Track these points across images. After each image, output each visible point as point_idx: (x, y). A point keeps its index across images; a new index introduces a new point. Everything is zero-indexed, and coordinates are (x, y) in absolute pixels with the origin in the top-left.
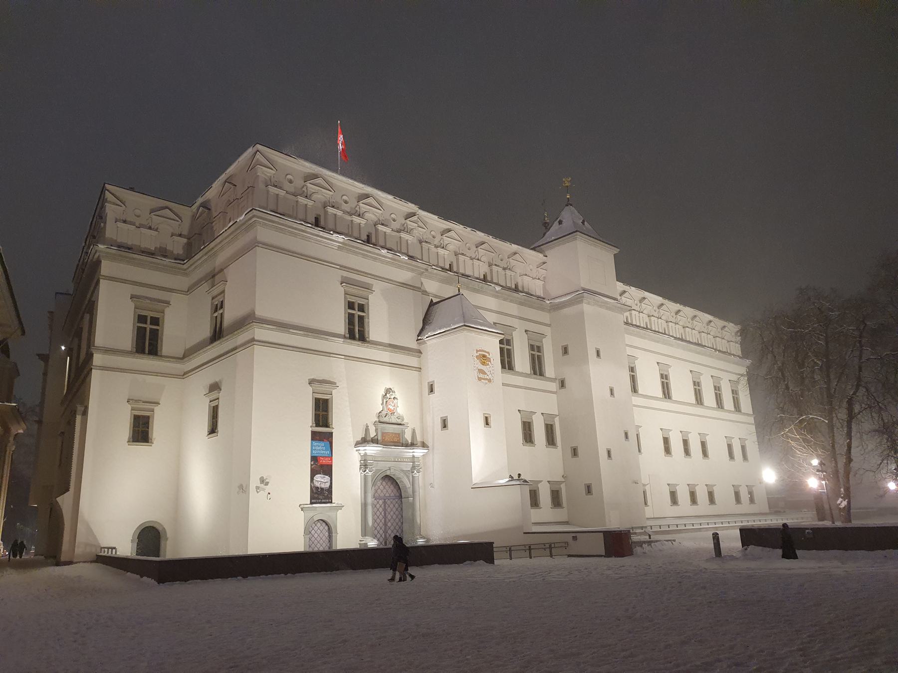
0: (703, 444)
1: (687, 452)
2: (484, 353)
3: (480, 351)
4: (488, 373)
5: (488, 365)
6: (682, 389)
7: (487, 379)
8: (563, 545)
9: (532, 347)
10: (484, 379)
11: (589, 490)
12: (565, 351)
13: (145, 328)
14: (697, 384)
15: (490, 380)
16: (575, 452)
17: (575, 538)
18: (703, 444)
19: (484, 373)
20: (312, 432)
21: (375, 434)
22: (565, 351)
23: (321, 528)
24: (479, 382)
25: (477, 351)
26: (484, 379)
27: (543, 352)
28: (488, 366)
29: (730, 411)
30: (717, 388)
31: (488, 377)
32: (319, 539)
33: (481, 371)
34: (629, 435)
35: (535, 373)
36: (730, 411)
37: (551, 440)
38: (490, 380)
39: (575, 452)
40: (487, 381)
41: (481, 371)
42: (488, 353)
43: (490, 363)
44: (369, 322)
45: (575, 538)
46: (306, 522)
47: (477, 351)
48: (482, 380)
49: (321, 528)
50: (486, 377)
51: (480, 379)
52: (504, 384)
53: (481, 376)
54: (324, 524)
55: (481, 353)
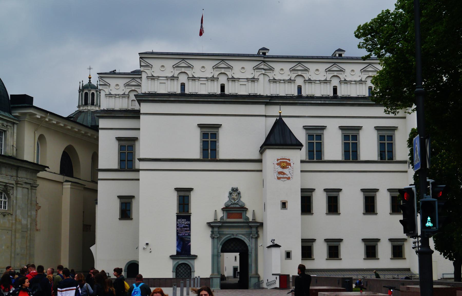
5: (288, 168)
15: (289, 178)
19: (284, 174)
20: (177, 215)
21: (222, 215)
23: (185, 267)
24: (278, 181)
25: (278, 160)
27: (395, 140)
28: (288, 169)
31: (287, 176)
32: (183, 273)
40: (286, 179)
42: (289, 160)
43: (289, 167)
44: (218, 145)
46: (174, 265)
47: (278, 160)
48: (282, 179)
50: (285, 176)
51: (279, 178)
53: (281, 176)
55: (280, 161)
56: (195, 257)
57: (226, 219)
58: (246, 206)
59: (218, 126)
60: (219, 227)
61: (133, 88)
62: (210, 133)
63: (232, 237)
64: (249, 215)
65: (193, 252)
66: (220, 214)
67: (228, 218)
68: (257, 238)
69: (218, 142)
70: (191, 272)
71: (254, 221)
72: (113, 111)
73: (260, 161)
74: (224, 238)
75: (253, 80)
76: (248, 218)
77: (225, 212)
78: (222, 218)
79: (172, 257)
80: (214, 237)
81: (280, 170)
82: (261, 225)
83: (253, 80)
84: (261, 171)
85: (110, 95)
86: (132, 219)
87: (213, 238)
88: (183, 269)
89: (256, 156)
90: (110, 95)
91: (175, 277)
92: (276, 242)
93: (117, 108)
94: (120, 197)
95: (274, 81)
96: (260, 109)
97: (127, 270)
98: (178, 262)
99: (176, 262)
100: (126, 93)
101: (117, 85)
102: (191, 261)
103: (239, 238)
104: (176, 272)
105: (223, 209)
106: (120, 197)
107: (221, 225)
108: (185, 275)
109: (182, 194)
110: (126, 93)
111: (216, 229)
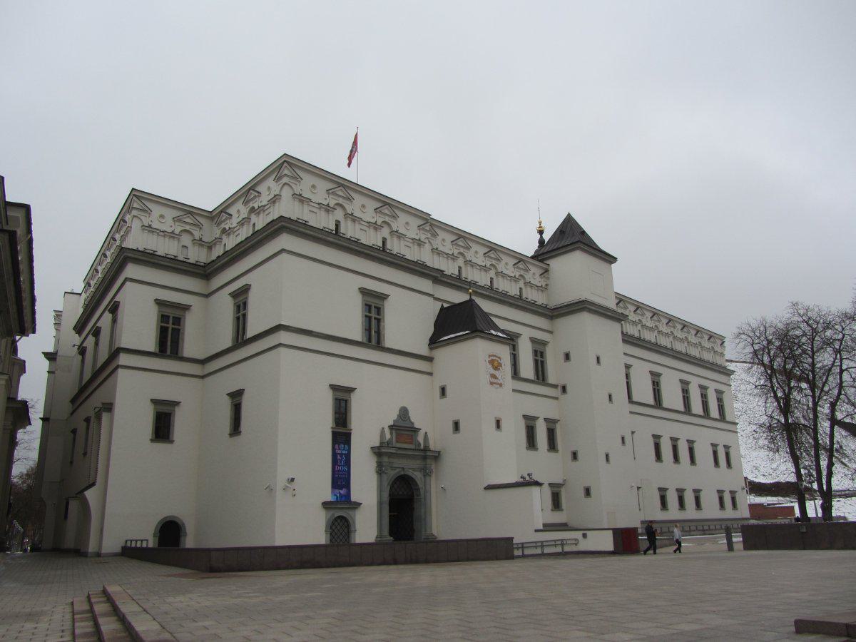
0: (691, 450)
1: (676, 458)
2: (497, 359)
3: (492, 356)
4: (500, 377)
6: (672, 397)
7: (498, 384)
8: (574, 542)
9: (535, 352)
10: (495, 383)
11: (588, 492)
12: (567, 357)
13: (173, 329)
14: (685, 392)
15: (501, 385)
16: (575, 456)
17: (585, 536)
18: (691, 450)
21: (389, 437)
22: (567, 357)
23: (341, 524)
26: (495, 383)
29: (716, 420)
30: (704, 397)
33: (493, 376)
34: (626, 440)
35: (538, 378)
36: (716, 420)
37: (552, 446)
38: (501, 385)
39: (575, 456)
41: (493, 376)
42: (499, 358)
45: (585, 536)
49: (341, 524)
51: (492, 383)
52: (514, 390)
53: (493, 380)
54: (343, 521)
55: (492, 358)
56: (358, 505)
57: (395, 444)
58: (416, 426)
59: (383, 297)
60: (390, 455)
61: (188, 228)
62: (373, 305)
63: (402, 473)
64: (420, 439)
65: (354, 498)
66: (388, 436)
67: (397, 442)
68: (430, 476)
69: (384, 322)
70: (348, 532)
71: (426, 449)
72: (153, 255)
73: (430, 359)
74: (392, 474)
75: (419, 243)
76: (420, 444)
77: (394, 432)
78: (391, 440)
79: (326, 505)
80: (384, 472)
81: (493, 371)
82: (437, 456)
83: (419, 243)
84: (430, 374)
85: (149, 229)
86: (172, 442)
87: (380, 470)
88: (339, 527)
89: (424, 351)
90: (149, 229)
91: (329, 542)
92: (535, 478)
93: (161, 253)
94: (154, 402)
95: (436, 251)
96: (425, 285)
97: (158, 535)
98: (333, 515)
99: (331, 513)
100: (177, 231)
101: (162, 216)
102: (351, 512)
103: (410, 474)
104: (331, 534)
105: (391, 427)
106: (153, 401)
107: (394, 451)
108: (341, 537)
109: (340, 395)
110: (177, 231)
111: (385, 459)
